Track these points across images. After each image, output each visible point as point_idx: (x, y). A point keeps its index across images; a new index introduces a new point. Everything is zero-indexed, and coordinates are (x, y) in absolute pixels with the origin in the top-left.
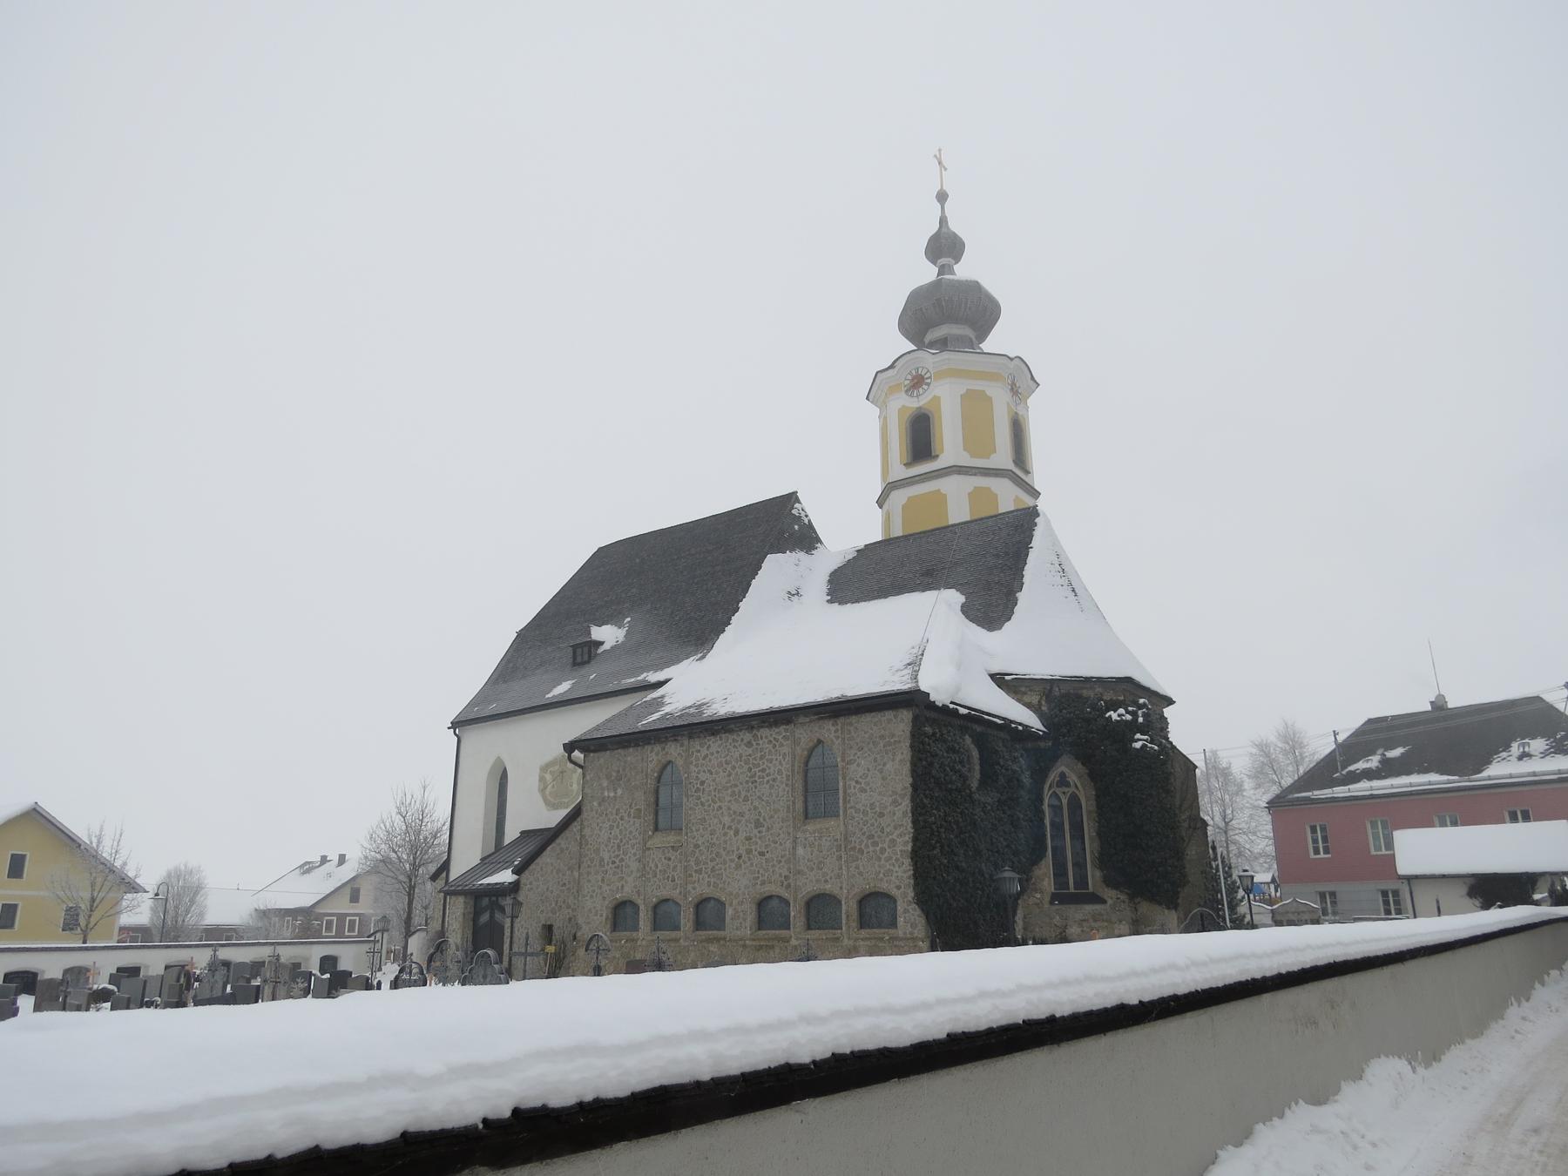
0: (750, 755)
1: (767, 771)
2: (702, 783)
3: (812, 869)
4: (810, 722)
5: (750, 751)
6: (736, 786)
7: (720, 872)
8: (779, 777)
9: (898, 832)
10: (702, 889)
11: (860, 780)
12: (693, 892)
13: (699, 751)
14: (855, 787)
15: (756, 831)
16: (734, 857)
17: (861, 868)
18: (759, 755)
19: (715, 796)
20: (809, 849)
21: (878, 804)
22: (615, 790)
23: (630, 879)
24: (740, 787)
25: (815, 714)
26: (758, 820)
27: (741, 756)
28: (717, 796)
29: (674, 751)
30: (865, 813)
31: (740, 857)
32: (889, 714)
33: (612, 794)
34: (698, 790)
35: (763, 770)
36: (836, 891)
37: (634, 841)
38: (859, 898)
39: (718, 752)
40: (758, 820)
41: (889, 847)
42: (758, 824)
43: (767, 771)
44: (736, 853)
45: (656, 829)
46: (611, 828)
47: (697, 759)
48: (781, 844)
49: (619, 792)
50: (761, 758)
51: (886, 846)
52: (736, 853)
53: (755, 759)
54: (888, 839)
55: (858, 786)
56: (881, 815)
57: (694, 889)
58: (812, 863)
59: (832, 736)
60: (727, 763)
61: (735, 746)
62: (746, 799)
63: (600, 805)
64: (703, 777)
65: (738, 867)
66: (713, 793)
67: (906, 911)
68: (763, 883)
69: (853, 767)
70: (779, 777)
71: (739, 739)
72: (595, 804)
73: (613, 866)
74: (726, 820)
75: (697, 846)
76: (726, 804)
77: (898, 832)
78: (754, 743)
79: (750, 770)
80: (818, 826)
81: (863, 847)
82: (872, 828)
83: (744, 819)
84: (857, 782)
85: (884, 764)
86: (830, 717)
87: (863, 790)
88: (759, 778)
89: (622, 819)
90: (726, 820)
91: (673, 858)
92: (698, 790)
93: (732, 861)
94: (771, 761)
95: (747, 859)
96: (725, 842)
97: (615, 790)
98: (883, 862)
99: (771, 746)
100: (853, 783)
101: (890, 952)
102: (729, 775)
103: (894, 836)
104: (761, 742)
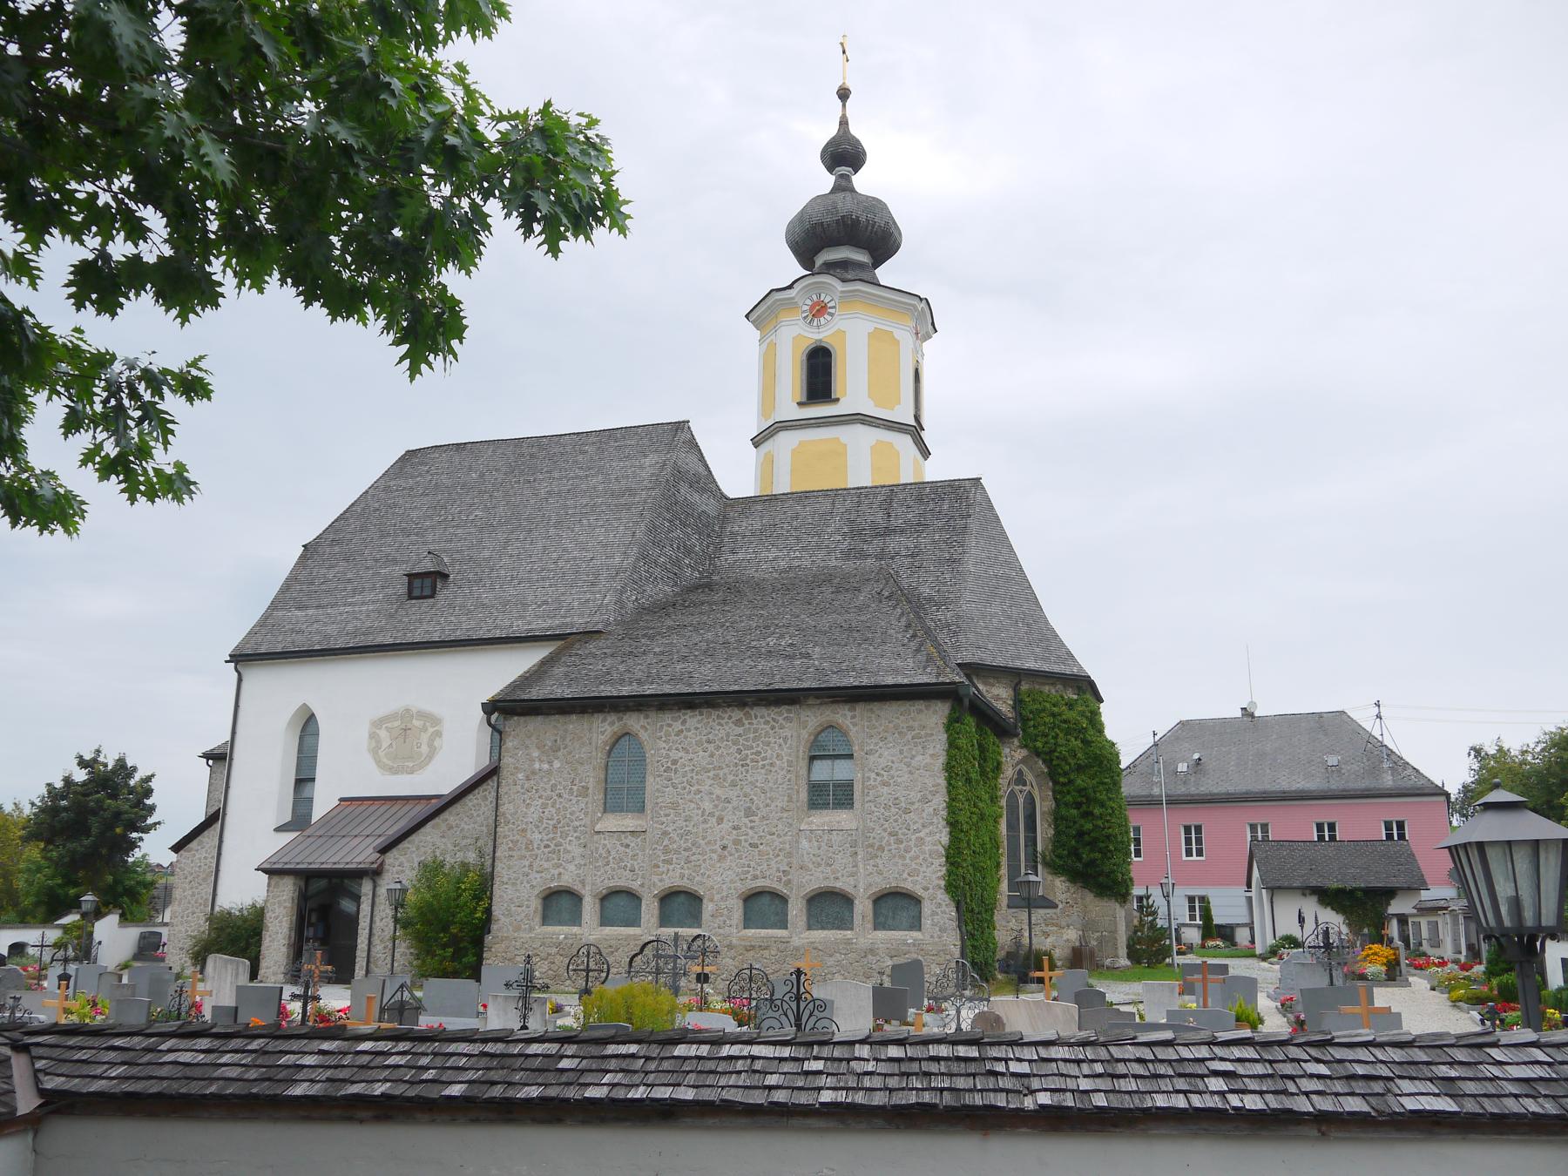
0: (740, 735)
1: (763, 755)
2: (675, 762)
3: (819, 865)
4: (821, 704)
5: (740, 730)
6: (721, 768)
7: (698, 863)
8: (778, 762)
9: (927, 831)
10: (673, 878)
11: (882, 772)
12: (659, 884)
13: (670, 725)
14: (875, 780)
15: (746, 820)
16: (717, 847)
17: (881, 867)
18: (752, 735)
19: (692, 778)
20: (816, 844)
21: (903, 799)
22: (550, 763)
23: (572, 867)
24: (726, 770)
25: (817, 697)
26: (749, 808)
27: (728, 735)
28: (695, 777)
29: (634, 722)
30: (887, 807)
31: (724, 848)
32: (920, 705)
33: (546, 766)
34: (667, 770)
35: (758, 753)
36: (849, 889)
37: (578, 823)
38: (875, 897)
39: (696, 729)
40: (749, 808)
41: (916, 846)
42: (749, 813)
43: (763, 755)
44: (719, 843)
45: (605, 811)
46: (544, 806)
47: (668, 735)
48: (779, 836)
49: (557, 764)
50: (754, 740)
51: (912, 843)
52: (719, 843)
53: (747, 740)
54: (914, 837)
55: (879, 779)
56: (907, 811)
57: (661, 881)
58: (819, 859)
59: (847, 722)
60: (709, 742)
61: (720, 724)
62: (733, 784)
63: (528, 779)
64: (674, 755)
65: (721, 858)
66: (690, 775)
67: (934, 913)
68: (755, 877)
69: (872, 758)
70: (778, 762)
71: (727, 716)
72: (520, 776)
73: (547, 850)
74: (707, 806)
75: (665, 833)
76: (706, 787)
77: (927, 831)
78: (746, 722)
79: (739, 751)
80: (827, 819)
81: (883, 843)
82: (895, 824)
83: (730, 806)
84: (878, 774)
85: (913, 757)
86: (846, 702)
87: (885, 784)
88: (752, 761)
89: (560, 796)
90: (707, 806)
91: (632, 845)
92: (667, 770)
93: (713, 851)
94: (768, 744)
95: (733, 851)
96: (705, 830)
97: (550, 763)
98: (908, 861)
99: (767, 727)
100: (873, 775)
101: (1538, 978)
102: (712, 756)
103: (922, 835)
104: (755, 722)
